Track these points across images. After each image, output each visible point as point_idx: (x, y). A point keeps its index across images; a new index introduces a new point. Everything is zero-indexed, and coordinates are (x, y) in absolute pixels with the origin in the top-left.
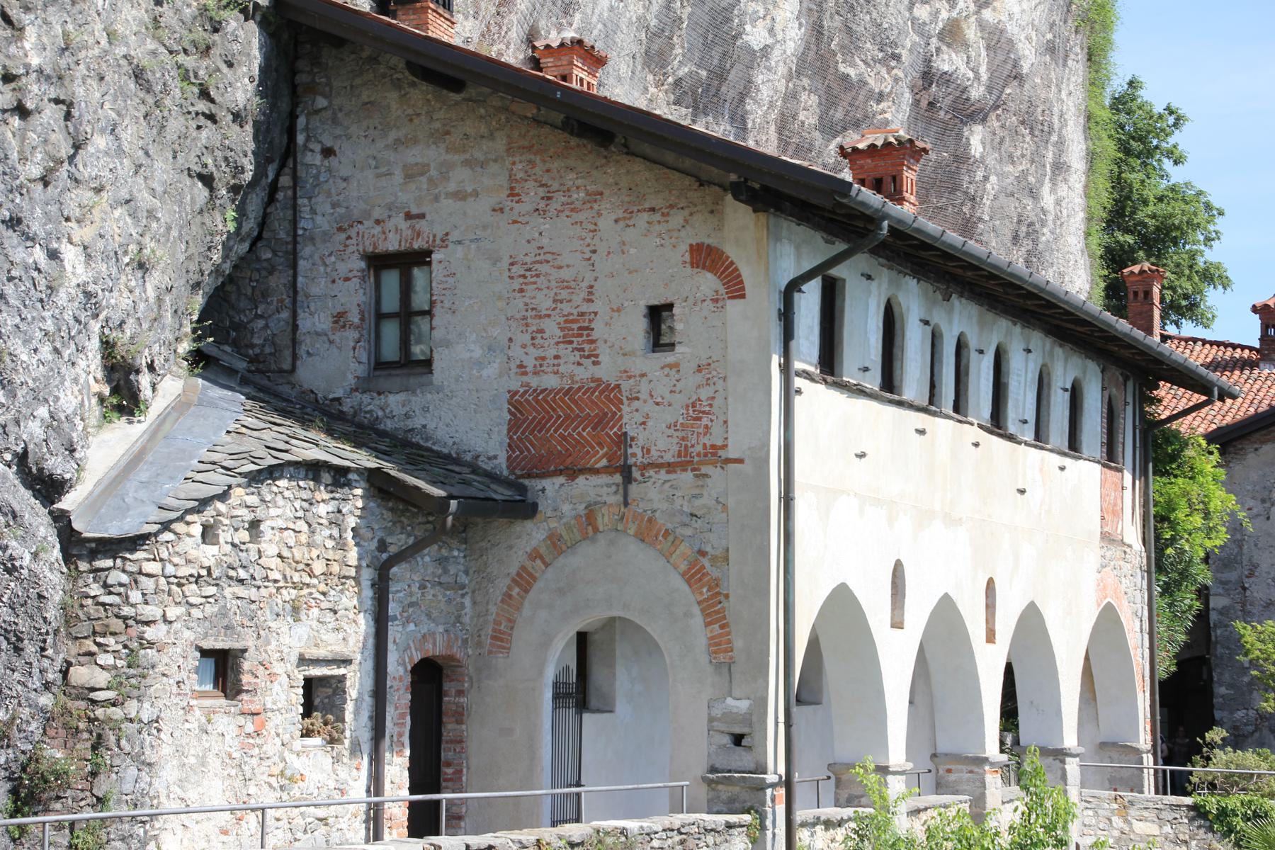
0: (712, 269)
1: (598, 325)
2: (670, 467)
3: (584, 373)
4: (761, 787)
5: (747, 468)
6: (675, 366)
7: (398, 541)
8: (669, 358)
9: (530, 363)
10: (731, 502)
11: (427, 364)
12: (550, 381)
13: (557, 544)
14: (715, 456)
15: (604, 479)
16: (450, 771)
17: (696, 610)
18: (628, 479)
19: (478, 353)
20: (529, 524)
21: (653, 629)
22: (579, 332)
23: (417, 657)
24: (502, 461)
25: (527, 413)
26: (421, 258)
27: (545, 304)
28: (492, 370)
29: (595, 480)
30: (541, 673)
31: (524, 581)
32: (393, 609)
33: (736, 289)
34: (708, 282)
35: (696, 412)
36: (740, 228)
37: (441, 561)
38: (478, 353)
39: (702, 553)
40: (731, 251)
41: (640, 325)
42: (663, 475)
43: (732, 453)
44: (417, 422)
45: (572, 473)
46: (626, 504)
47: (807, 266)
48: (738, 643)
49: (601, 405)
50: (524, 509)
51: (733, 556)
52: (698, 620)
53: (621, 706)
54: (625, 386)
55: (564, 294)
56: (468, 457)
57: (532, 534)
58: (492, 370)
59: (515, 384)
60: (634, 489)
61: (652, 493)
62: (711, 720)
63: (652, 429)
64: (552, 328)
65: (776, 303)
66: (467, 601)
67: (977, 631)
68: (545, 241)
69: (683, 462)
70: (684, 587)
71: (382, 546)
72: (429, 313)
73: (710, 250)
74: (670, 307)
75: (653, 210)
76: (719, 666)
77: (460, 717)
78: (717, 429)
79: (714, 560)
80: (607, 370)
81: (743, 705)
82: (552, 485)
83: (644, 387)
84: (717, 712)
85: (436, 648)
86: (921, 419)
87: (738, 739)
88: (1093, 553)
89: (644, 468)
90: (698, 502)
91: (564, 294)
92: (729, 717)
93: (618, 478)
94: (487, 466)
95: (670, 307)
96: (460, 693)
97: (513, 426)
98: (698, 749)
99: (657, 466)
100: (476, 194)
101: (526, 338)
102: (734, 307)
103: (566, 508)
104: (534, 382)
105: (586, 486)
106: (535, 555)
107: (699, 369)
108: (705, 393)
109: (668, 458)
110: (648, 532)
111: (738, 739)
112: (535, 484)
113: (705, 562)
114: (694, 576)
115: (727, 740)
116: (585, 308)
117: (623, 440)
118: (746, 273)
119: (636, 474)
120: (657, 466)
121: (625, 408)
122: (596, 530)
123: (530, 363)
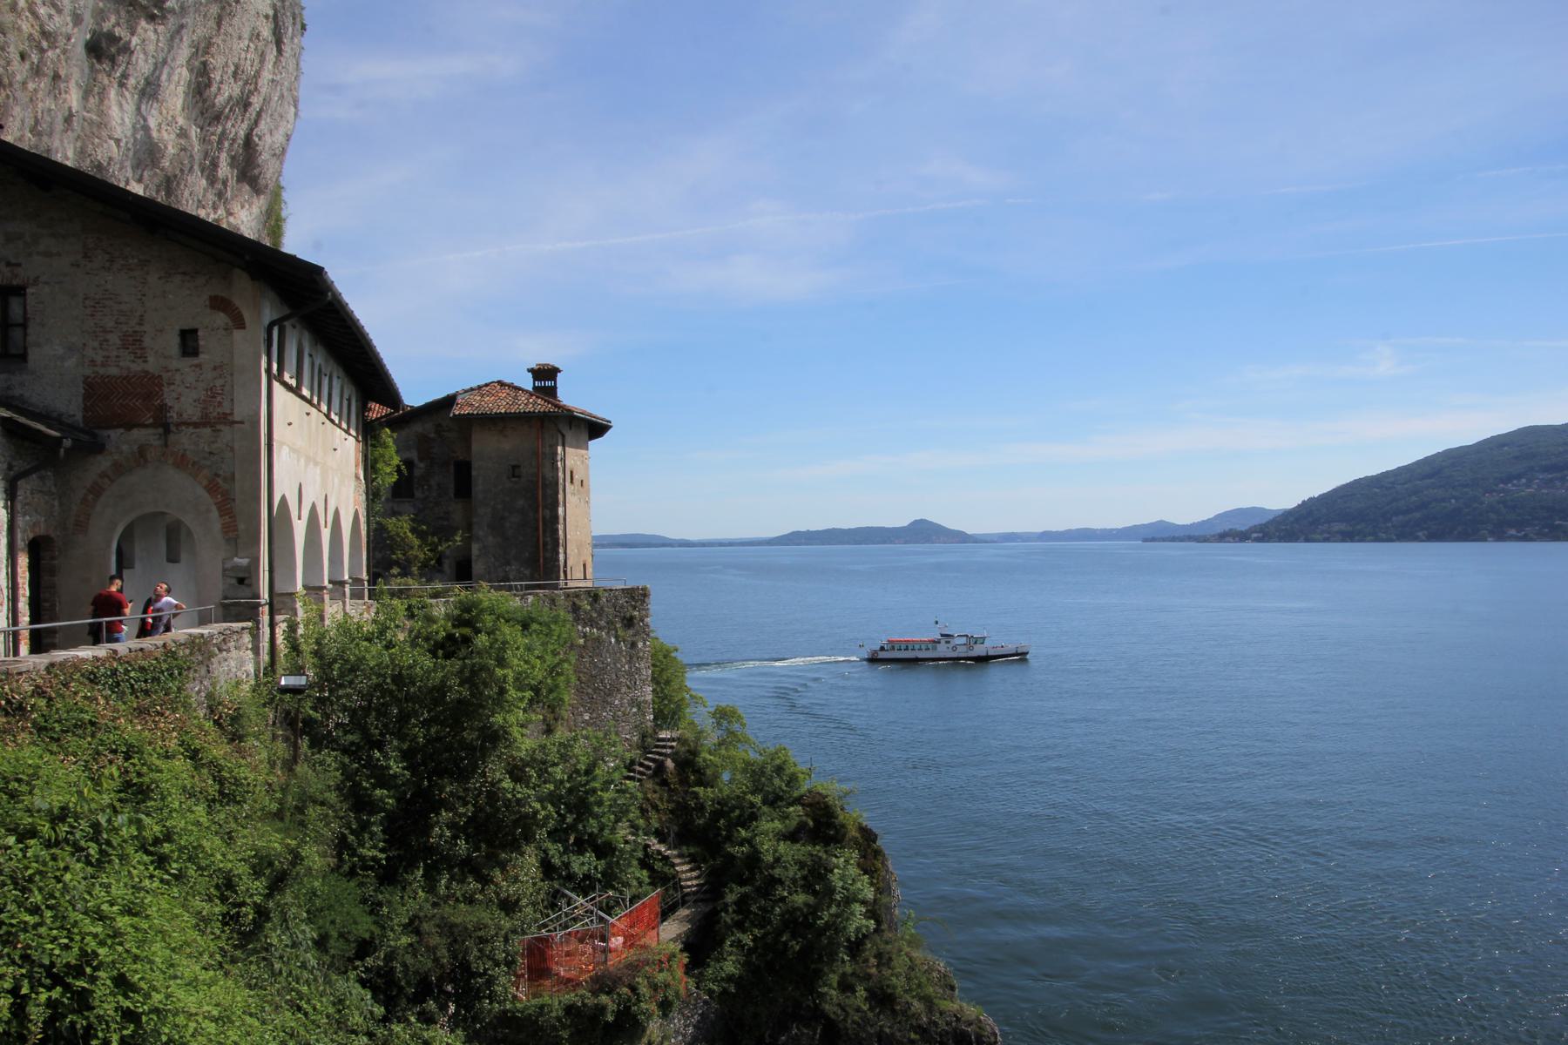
0: (224, 311)
1: (147, 341)
2: (196, 425)
3: (137, 367)
4: (259, 605)
5: (246, 426)
6: (199, 366)
7: (20, 465)
8: (195, 361)
9: (99, 359)
10: (236, 446)
11: (23, 357)
12: (113, 371)
13: (119, 469)
14: (226, 419)
15: (151, 431)
16: (47, 605)
17: (214, 508)
18: (167, 431)
19: (61, 351)
20: (99, 457)
21: (188, 520)
22: (133, 342)
23: (31, 536)
24: (79, 417)
25: (95, 390)
26: (20, 291)
27: (110, 324)
28: (70, 363)
29: (144, 431)
30: (109, 546)
31: (97, 491)
32: (19, 507)
33: (239, 323)
34: (221, 319)
35: (212, 393)
36: (242, 290)
37: (42, 478)
38: (61, 351)
39: (217, 475)
40: (237, 302)
41: (174, 342)
42: (191, 429)
43: (237, 418)
44: (17, 392)
45: (129, 426)
46: (166, 445)
47: (275, 317)
48: (241, 527)
49: (149, 388)
50: (98, 448)
51: (237, 476)
52: (215, 514)
53: (138, 565)
54: (165, 376)
55: (122, 319)
56: (55, 415)
57: (103, 463)
58: (70, 363)
59: (88, 371)
60: (172, 438)
61: (185, 440)
62: (224, 570)
63: (184, 400)
64: (114, 339)
65: (263, 335)
66: (56, 503)
67: (322, 522)
68: (109, 286)
69: (205, 422)
70: (206, 495)
71: (10, 467)
72: (24, 326)
73: (223, 299)
74: (195, 331)
75: (184, 273)
76: (228, 540)
77: (53, 572)
78: (226, 404)
79: (225, 480)
80: (152, 365)
81: (245, 562)
82: (115, 434)
83: (178, 377)
84: (228, 565)
85: (41, 531)
86: (307, 407)
87: (241, 581)
88: (353, 483)
89: (178, 425)
90: (214, 446)
91: (122, 319)
92: (236, 568)
93: (161, 430)
94: (69, 421)
95: (195, 331)
96: (53, 558)
97: (86, 397)
98: (217, 587)
99: (187, 424)
100: (59, 254)
101: (96, 344)
102: (238, 335)
103: (125, 448)
104: (102, 371)
105: (137, 434)
106: (103, 475)
107: (215, 368)
108: (219, 383)
109: (195, 419)
110: (182, 462)
111: (241, 581)
112: (105, 433)
113: (220, 480)
114: (212, 488)
115: (234, 581)
116: (137, 328)
117: (163, 408)
118: (247, 315)
119: (173, 428)
120: (187, 424)
121: (165, 389)
122: (146, 461)
123: (99, 359)
